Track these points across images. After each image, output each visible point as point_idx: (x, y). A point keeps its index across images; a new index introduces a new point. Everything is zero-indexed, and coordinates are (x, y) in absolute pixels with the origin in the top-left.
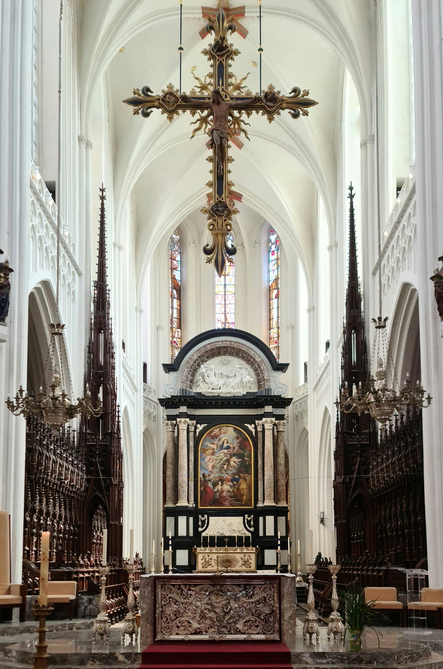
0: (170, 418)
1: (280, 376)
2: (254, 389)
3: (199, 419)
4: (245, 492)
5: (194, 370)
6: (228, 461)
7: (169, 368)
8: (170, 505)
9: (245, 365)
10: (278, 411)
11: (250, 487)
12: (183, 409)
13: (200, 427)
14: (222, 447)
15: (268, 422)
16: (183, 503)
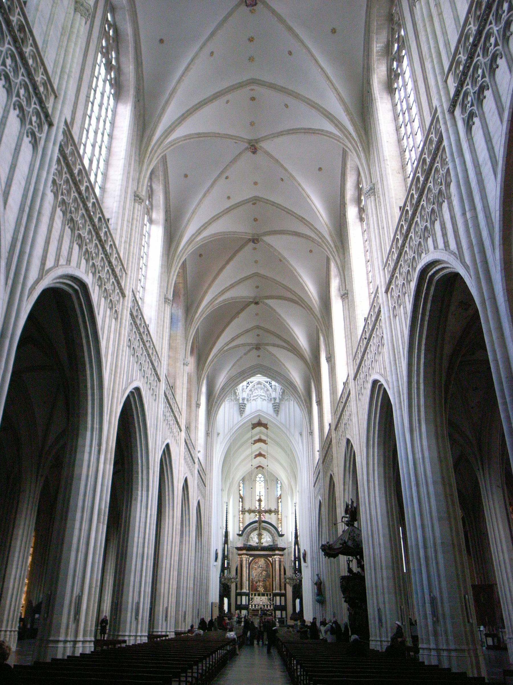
0: (239, 555)
1: (281, 538)
2: (272, 544)
3: (251, 555)
4: (268, 586)
5: (248, 536)
6: (261, 573)
7: (239, 535)
8: (238, 591)
9: (268, 534)
10: (281, 553)
11: (270, 584)
12: (244, 552)
13: (251, 559)
14: (259, 567)
15: (277, 558)
16: (244, 590)
